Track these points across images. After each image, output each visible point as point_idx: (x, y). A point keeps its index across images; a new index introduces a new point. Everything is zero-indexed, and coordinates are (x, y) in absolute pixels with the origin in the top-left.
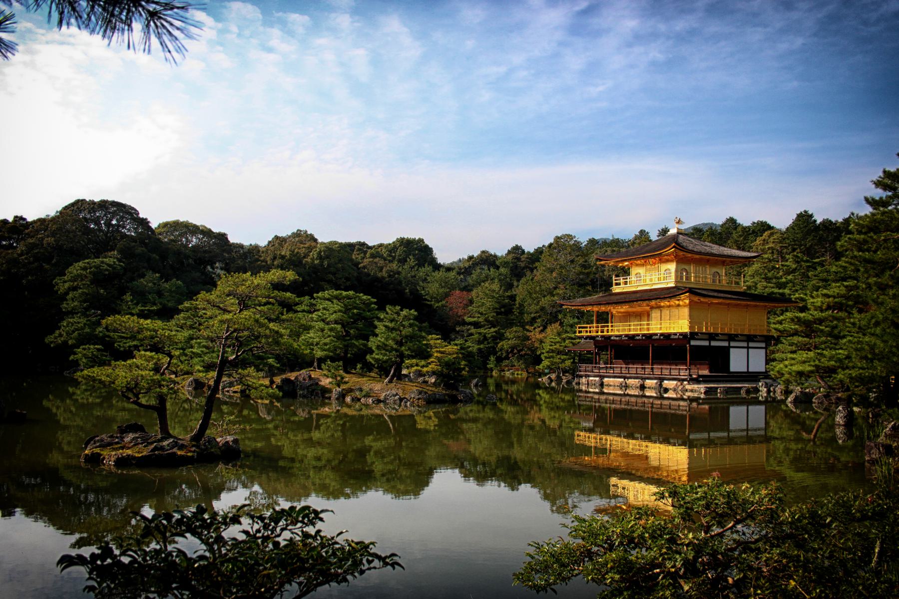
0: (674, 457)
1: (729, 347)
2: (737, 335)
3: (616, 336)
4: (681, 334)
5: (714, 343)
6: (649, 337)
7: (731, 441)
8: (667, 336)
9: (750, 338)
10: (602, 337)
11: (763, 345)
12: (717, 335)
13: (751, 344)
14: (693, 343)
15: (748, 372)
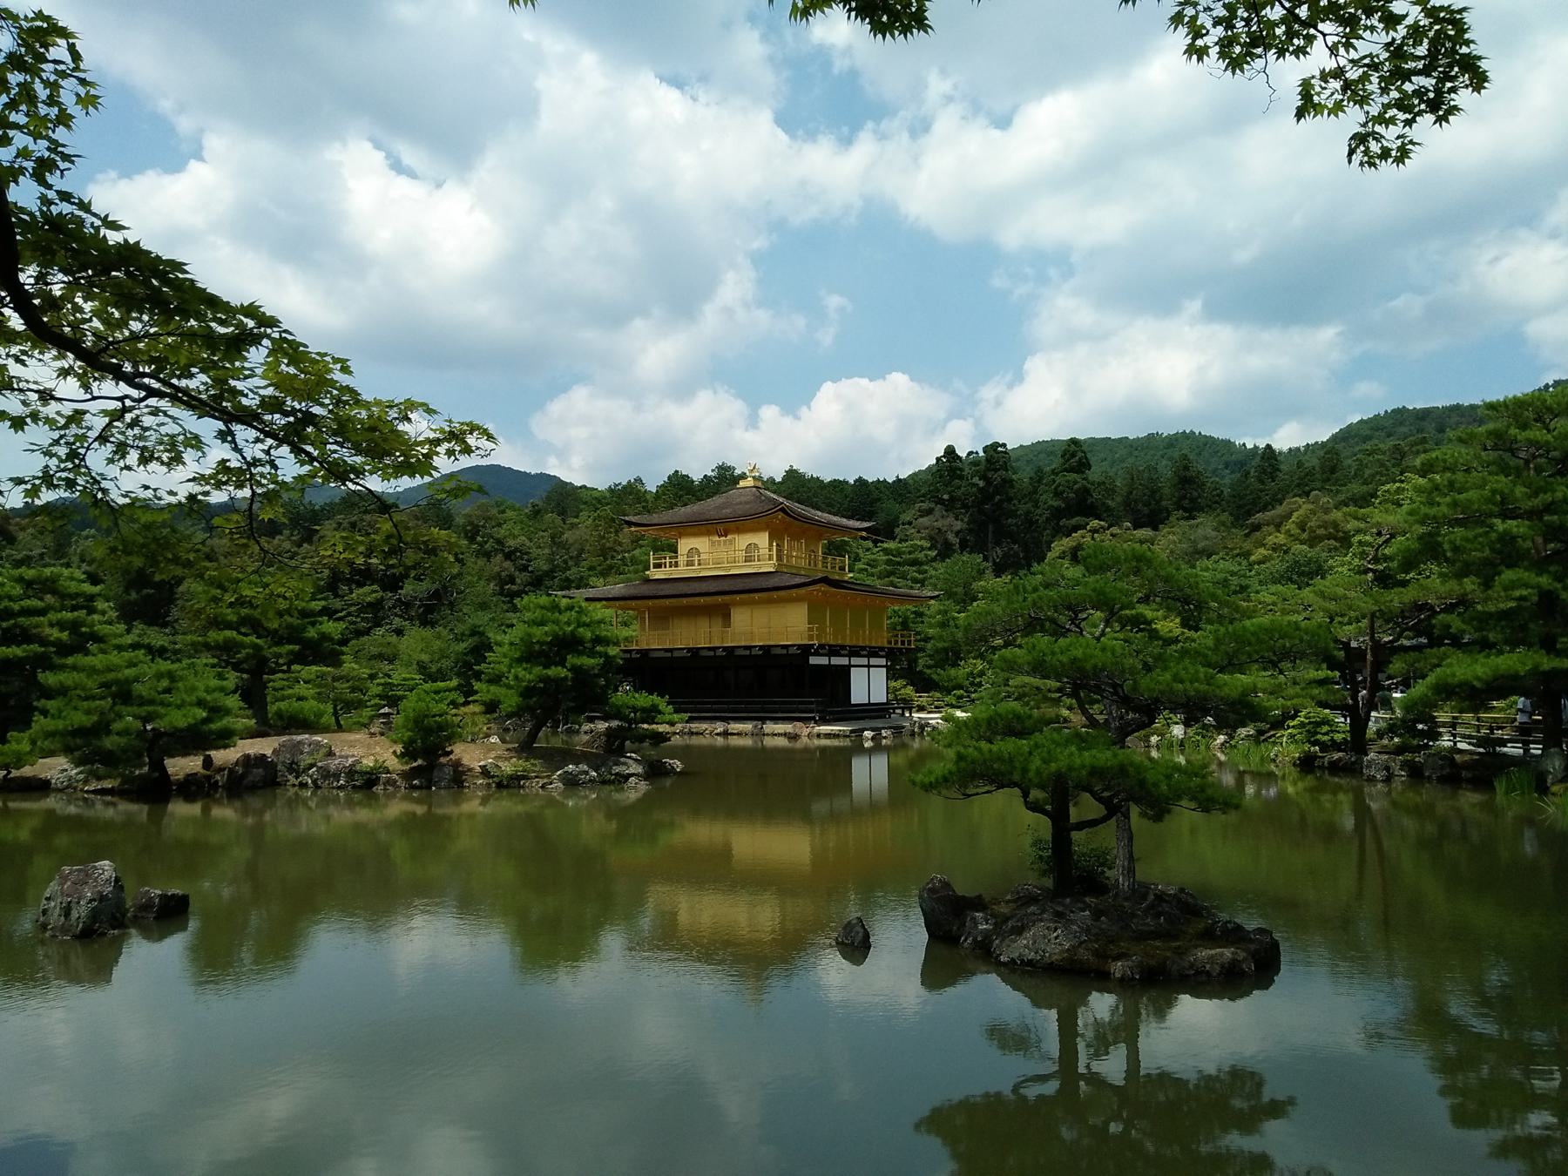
0: (786, 845)
1: (850, 666)
2: (863, 648)
3: (666, 650)
4: (799, 646)
5: (836, 661)
6: (730, 650)
7: (856, 813)
8: (766, 649)
9: (873, 652)
10: (638, 651)
11: (883, 661)
12: (843, 647)
13: (874, 661)
14: (813, 660)
15: (869, 704)
